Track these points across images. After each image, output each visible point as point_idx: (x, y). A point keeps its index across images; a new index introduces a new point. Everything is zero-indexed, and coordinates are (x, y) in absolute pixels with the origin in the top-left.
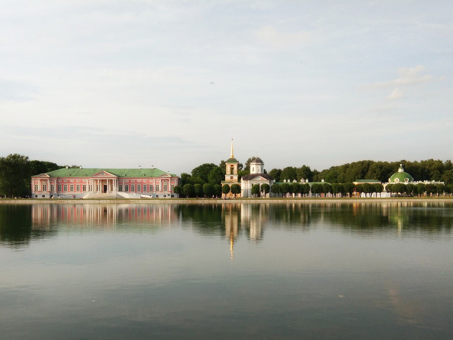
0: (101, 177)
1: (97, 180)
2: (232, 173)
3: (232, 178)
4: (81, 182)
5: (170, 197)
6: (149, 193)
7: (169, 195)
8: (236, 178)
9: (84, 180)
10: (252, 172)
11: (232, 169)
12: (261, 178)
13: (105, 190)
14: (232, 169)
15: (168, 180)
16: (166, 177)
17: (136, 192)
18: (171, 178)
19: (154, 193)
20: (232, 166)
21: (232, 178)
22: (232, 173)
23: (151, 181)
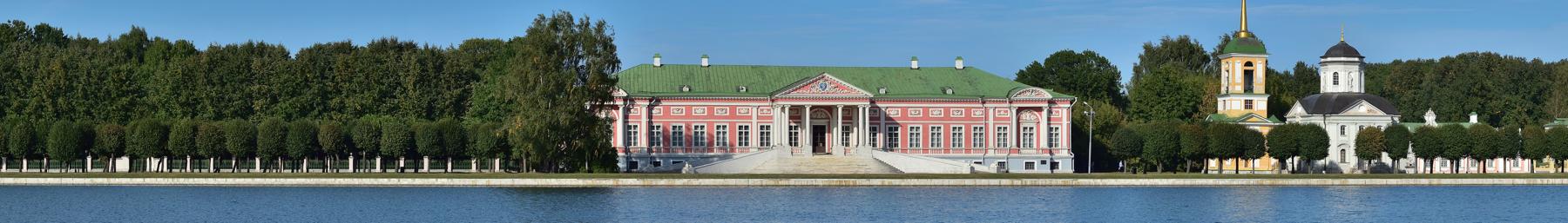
0: (809, 97)
1: (803, 107)
2: (1248, 88)
3: (1249, 104)
4: (733, 115)
5: (1046, 169)
6: (972, 154)
7: (1044, 162)
8: (1261, 104)
9: (742, 107)
10: (1327, 86)
11: (1249, 75)
12: (1364, 108)
13: (818, 143)
14: (1249, 75)
15: (1039, 109)
16: (1034, 96)
17: (925, 151)
18: (1051, 102)
19: (991, 153)
20: (1249, 64)
21: (1249, 104)
22: (1248, 88)
23: (979, 113)
